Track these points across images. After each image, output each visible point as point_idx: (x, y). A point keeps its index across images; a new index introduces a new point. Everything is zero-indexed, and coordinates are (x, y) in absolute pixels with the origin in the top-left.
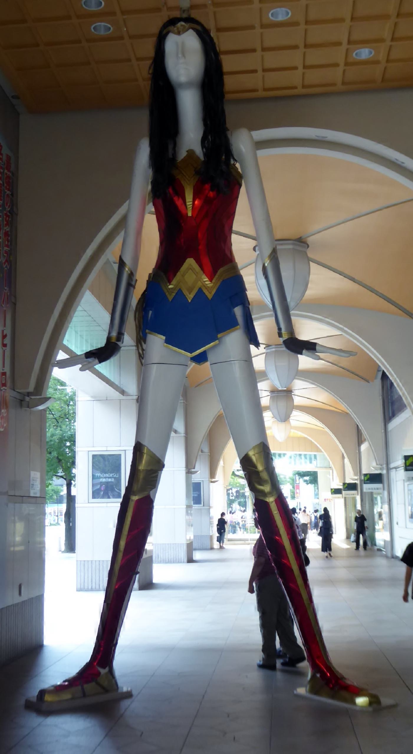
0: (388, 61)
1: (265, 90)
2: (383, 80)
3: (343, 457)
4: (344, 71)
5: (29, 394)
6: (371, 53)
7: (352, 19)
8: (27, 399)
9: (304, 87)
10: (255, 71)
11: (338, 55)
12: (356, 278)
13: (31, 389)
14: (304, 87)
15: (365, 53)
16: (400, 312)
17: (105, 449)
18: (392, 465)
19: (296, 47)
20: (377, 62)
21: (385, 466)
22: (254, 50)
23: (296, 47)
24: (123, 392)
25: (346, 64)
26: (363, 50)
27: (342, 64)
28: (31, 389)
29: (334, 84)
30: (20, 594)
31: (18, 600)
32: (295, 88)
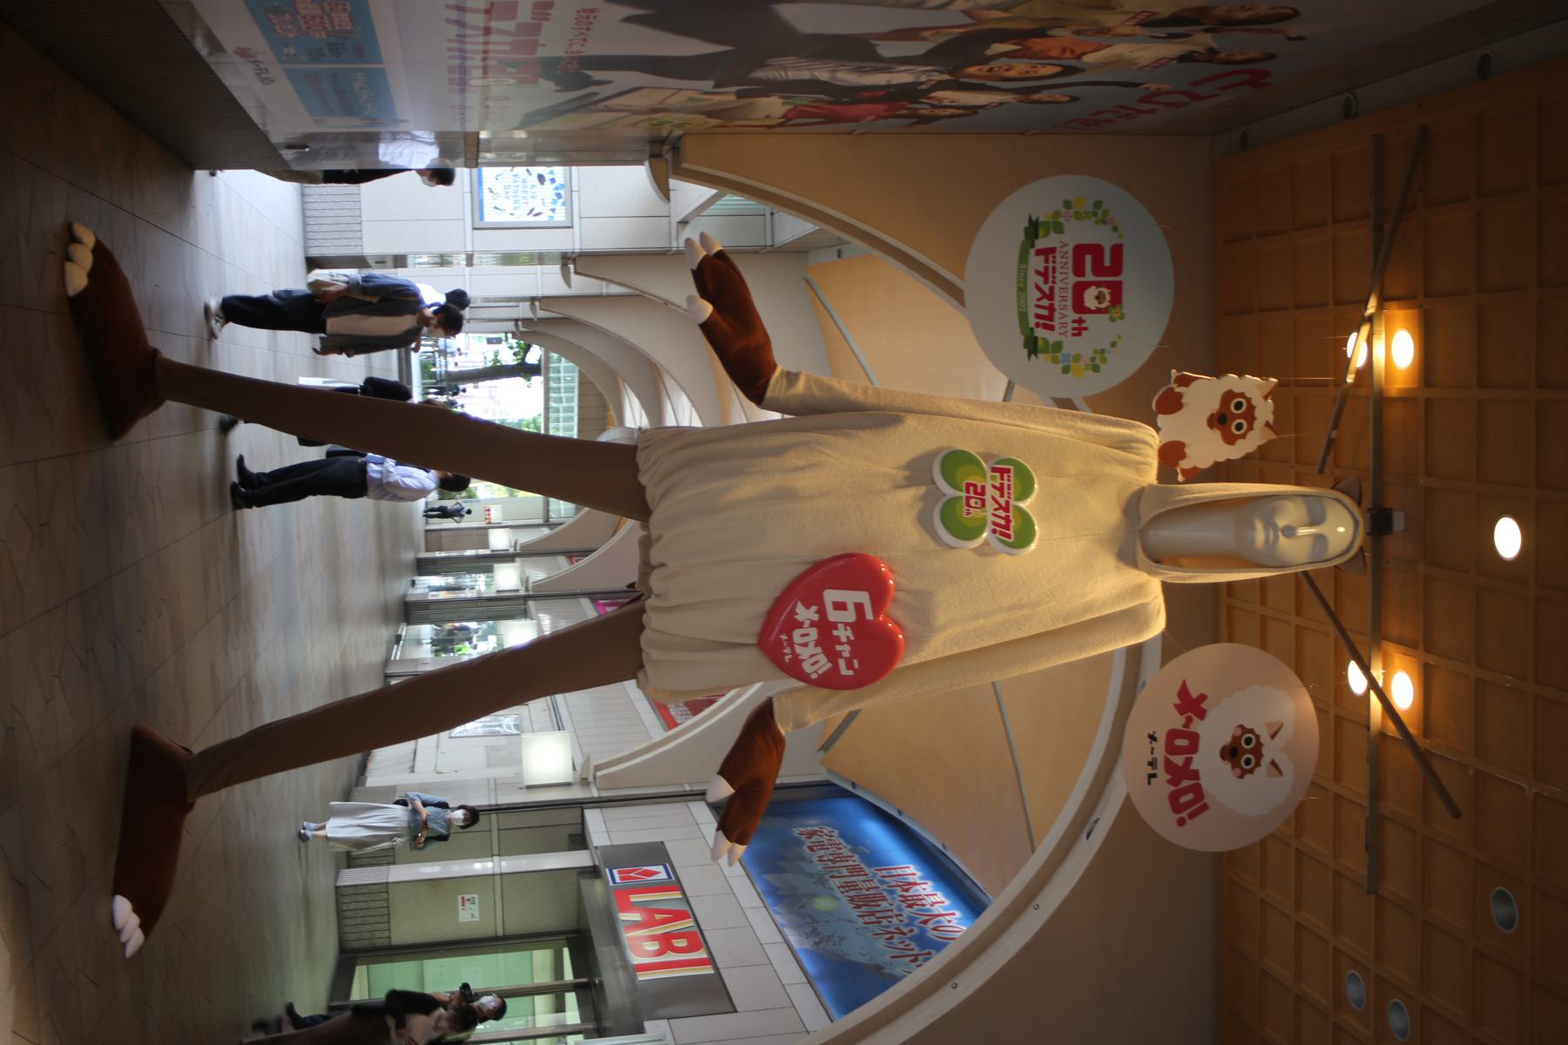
3: (571, 555)
7: (1337, 796)
13: (684, 165)
22: (1299, 613)
24: (684, 223)
28: (684, 165)
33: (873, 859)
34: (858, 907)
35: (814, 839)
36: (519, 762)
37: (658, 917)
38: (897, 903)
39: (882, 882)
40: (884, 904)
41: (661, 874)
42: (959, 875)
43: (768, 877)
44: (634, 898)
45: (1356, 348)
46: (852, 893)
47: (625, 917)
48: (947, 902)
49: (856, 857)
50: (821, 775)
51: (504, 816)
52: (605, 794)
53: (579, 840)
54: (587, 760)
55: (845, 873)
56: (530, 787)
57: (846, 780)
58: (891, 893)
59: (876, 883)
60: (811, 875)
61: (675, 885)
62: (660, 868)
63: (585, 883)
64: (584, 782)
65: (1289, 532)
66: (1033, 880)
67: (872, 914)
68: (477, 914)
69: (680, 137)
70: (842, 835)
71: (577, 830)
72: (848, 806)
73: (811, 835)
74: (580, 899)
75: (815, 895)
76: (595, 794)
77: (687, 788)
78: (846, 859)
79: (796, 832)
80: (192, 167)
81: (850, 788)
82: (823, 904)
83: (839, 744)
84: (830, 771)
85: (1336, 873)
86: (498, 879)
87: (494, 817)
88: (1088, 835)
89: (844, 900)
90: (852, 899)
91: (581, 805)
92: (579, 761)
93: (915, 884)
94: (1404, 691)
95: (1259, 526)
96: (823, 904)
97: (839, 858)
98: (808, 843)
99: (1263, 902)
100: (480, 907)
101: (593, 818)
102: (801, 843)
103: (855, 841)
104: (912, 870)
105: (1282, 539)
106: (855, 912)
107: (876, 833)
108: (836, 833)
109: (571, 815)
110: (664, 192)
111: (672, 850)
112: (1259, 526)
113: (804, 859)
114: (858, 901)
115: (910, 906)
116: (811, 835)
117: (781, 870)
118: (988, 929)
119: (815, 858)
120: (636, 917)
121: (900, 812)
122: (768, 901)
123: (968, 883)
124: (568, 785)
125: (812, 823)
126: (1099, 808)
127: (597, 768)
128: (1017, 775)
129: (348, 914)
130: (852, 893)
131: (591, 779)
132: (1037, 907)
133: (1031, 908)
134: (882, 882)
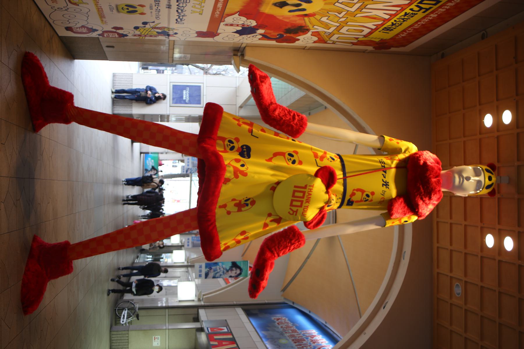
0: (451, 304)
1: (438, 222)
2: (438, 299)
4: (448, 276)
5: (243, 55)
6: (458, 294)
7: (482, 287)
8: (239, 54)
9: (438, 248)
10: (451, 218)
11: (458, 273)
12: (308, 260)
14: (438, 248)
15: (458, 290)
16: (285, 284)
17: (205, 94)
18: (190, 269)
19: (465, 247)
20: (451, 298)
21: (190, 264)
22: (465, 219)
23: (465, 247)
24: (241, 107)
25: (451, 278)
26: (460, 289)
27: (452, 275)
28: (246, 58)
29: (438, 267)
30: (107, 47)
31: (104, 45)
32: (438, 242)
33: (300, 328)
34: (295, 343)
35: (279, 321)
36: (177, 294)
37: (224, 343)
38: (309, 341)
39: (304, 335)
40: (304, 342)
41: (226, 330)
42: (332, 333)
43: (263, 332)
44: (216, 337)
45: (488, 121)
46: (293, 338)
47: (212, 343)
48: (327, 342)
49: (294, 327)
50: (282, 300)
51: (170, 310)
52: (206, 304)
53: (197, 319)
54: (201, 292)
55: (290, 331)
56: (180, 301)
57: (290, 301)
58: (307, 338)
59: (301, 335)
60: (278, 332)
61: (231, 333)
62: (225, 328)
63: (198, 333)
64: (199, 300)
65: (468, 179)
66: (364, 323)
67: (301, 345)
68: (159, 343)
69: (245, 47)
70: (289, 320)
71: (196, 316)
72: (291, 311)
73: (278, 319)
74: (196, 339)
75: (279, 338)
76: (202, 303)
77: (235, 303)
78: (291, 327)
79: (273, 318)
80: (74, 59)
81: (292, 304)
82: (283, 341)
83: (288, 289)
84: (285, 299)
85: (481, 316)
86: (167, 331)
87: (167, 310)
88: (384, 308)
89: (290, 340)
90: (293, 340)
91: (197, 307)
92: (198, 293)
93: (315, 336)
94: (509, 244)
95: (457, 177)
96: (283, 341)
97: (288, 327)
98: (277, 322)
99: (451, 331)
100: (161, 340)
101: (202, 312)
102: (275, 322)
103: (294, 322)
104: (313, 331)
105: (465, 181)
106: (294, 345)
107: (301, 320)
108: (287, 319)
109: (194, 311)
110: (238, 70)
111: (228, 321)
112: (457, 177)
113: (275, 327)
114: (296, 341)
115: (314, 343)
116: (278, 319)
117: (268, 330)
118: (346, 343)
119: (280, 327)
120: (216, 343)
121: (310, 312)
122: (264, 339)
123: (335, 336)
124: (193, 301)
125: (278, 316)
126: (388, 298)
127: (204, 295)
128: (355, 292)
129: (114, 341)
130: (293, 338)
131: (201, 299)
132: (365, 334)
133: (363, 334)
134: (304, 335)
